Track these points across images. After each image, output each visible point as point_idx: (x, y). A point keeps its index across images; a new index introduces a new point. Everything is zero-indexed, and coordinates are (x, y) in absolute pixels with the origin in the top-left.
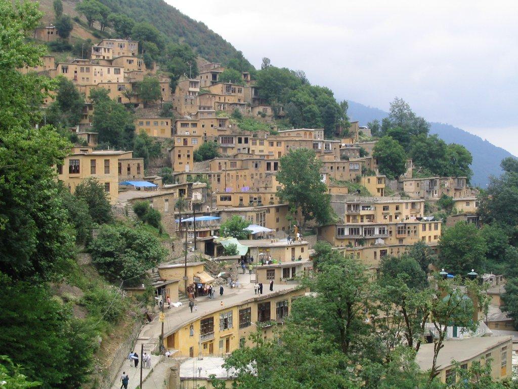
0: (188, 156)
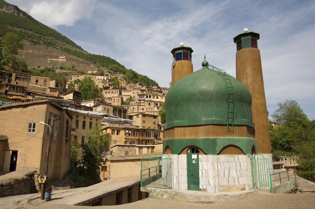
0: (119, 101)
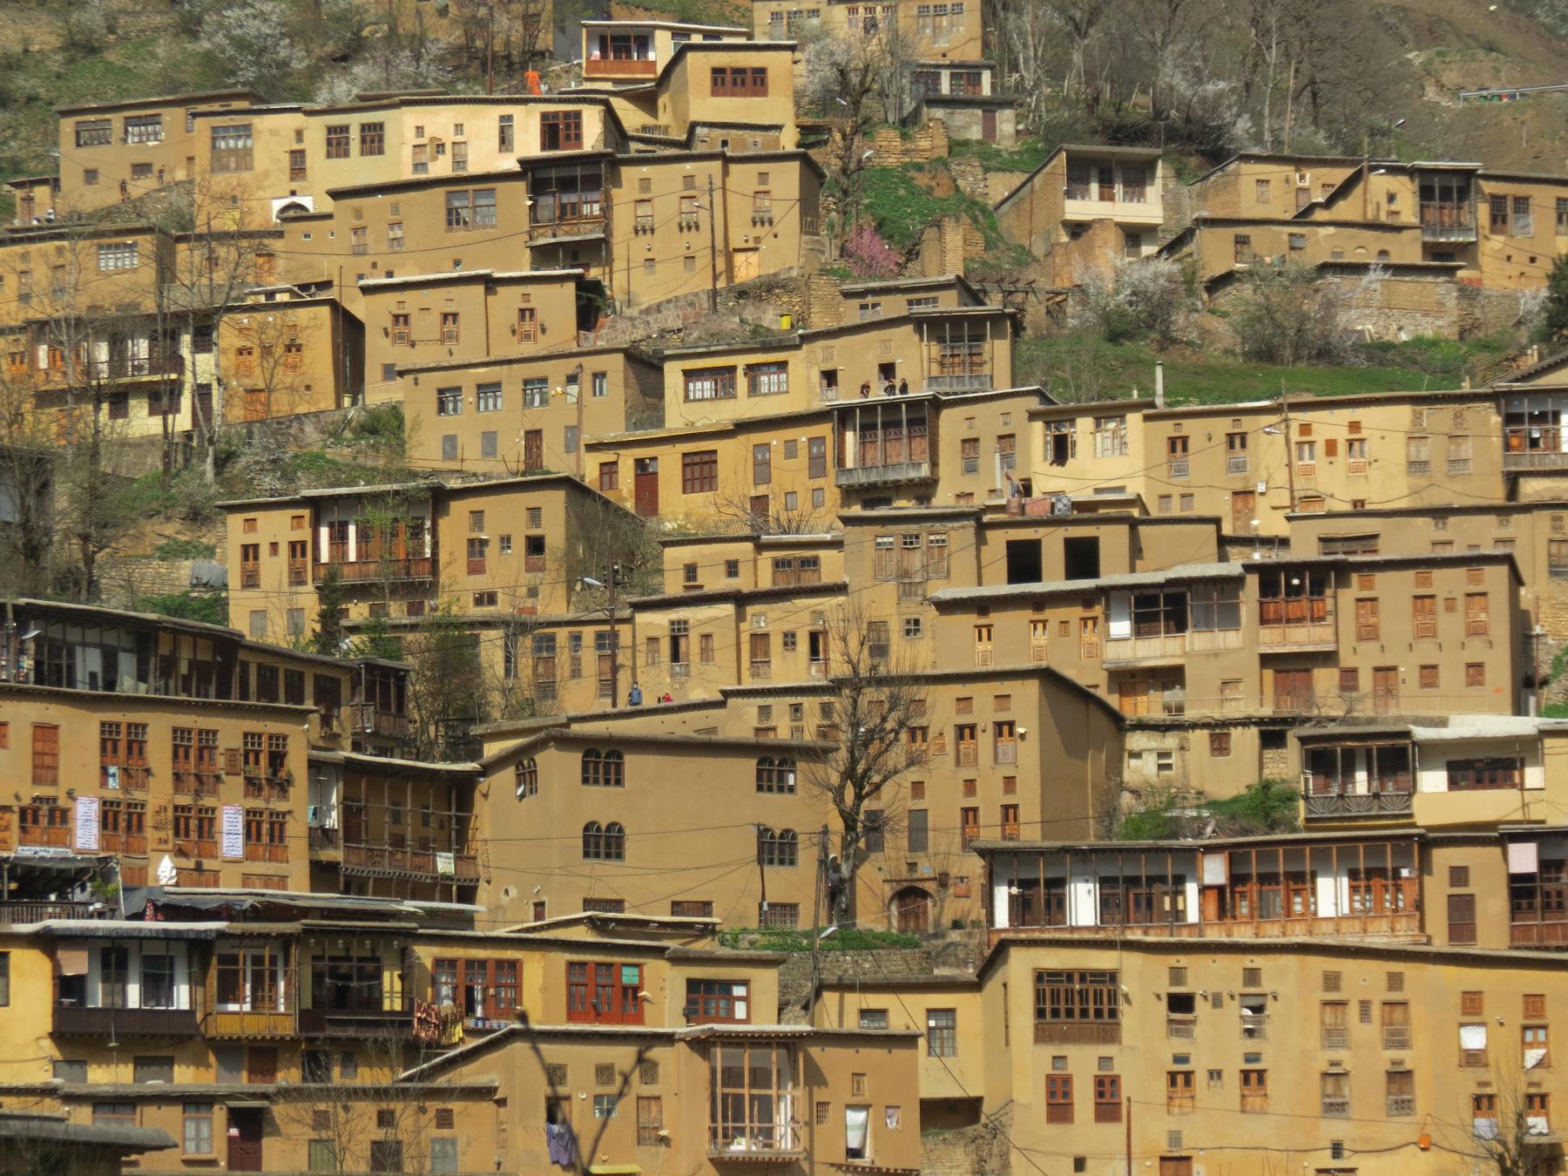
0: (536, 545)
